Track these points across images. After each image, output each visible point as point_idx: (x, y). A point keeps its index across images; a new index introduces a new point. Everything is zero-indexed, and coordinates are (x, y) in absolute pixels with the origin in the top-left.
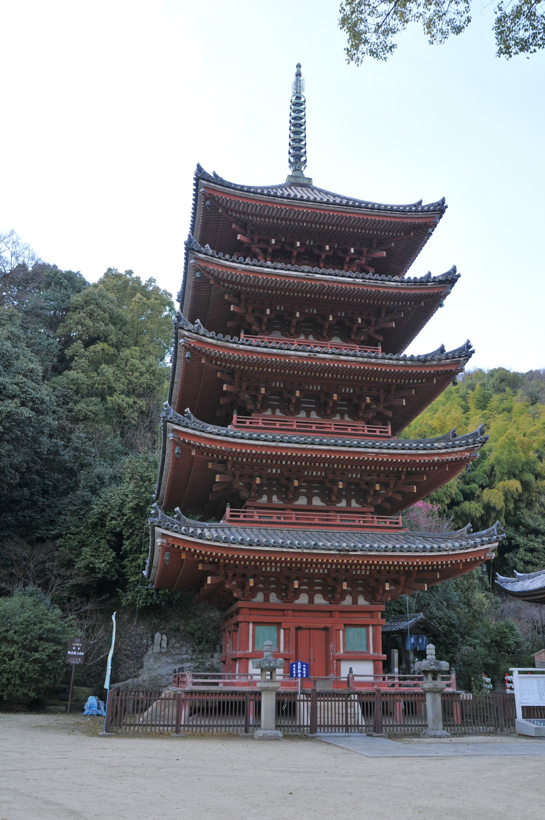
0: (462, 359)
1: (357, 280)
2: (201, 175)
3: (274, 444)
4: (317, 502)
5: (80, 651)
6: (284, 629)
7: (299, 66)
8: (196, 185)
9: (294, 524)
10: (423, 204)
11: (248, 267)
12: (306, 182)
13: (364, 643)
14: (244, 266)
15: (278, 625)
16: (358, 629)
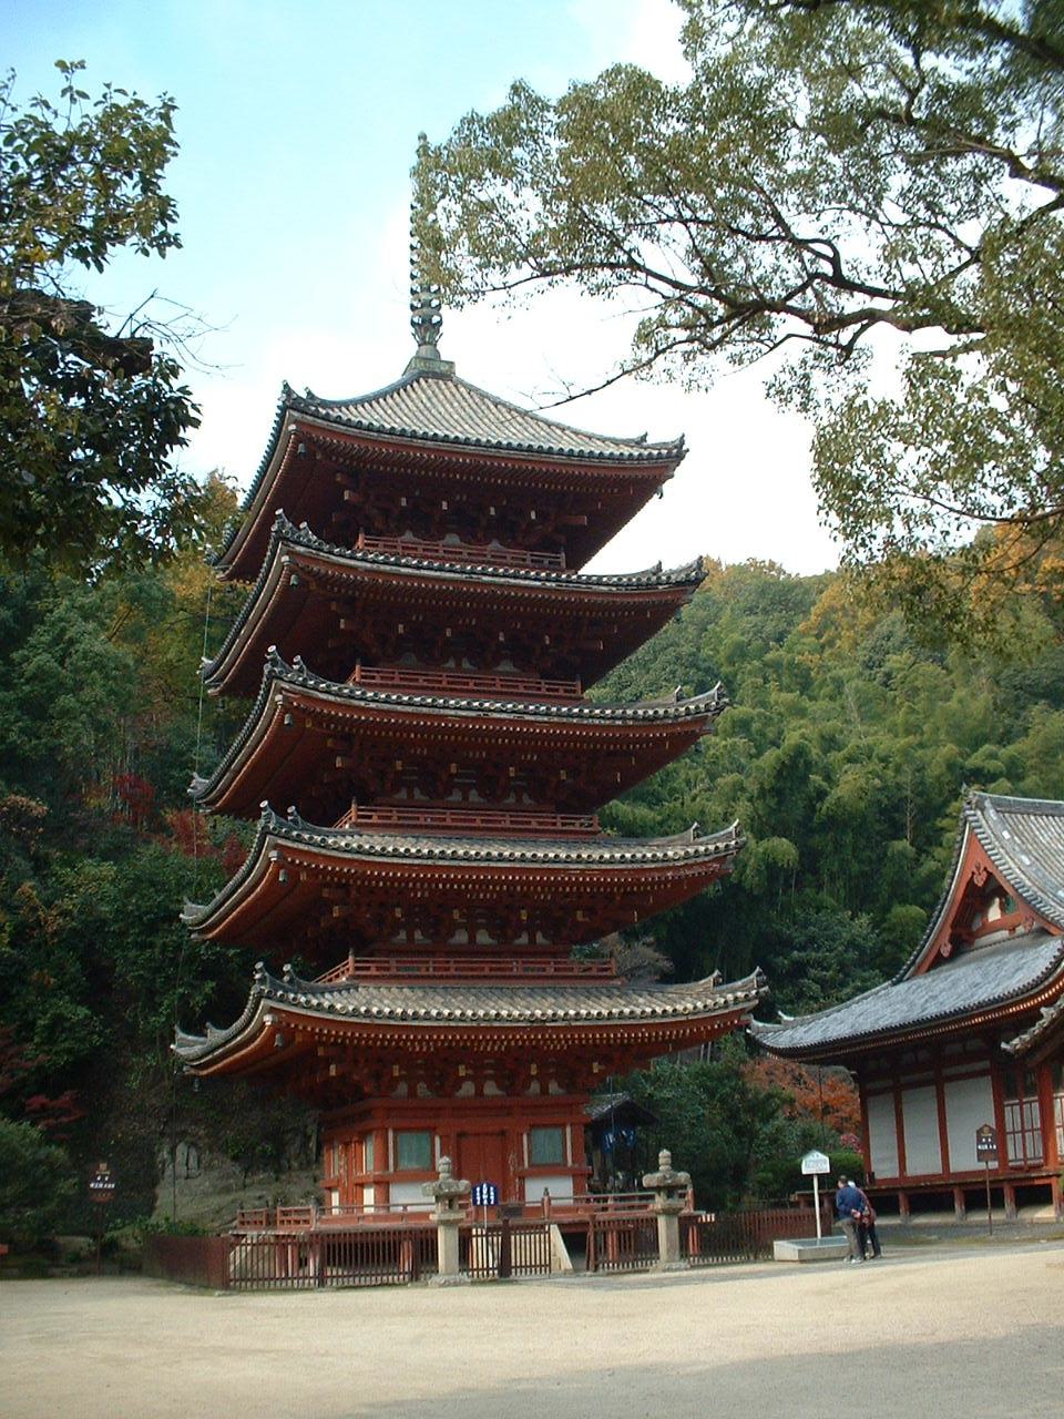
0: (710, 714)
1: (548, 584)
2: (294, 405)
3: (430, 862)
4: (483, 938)
5: (108, 1182)
6: (441, 1138)
8: (282, 416)
9: (454, 977)
10: (650, 441)
11: (375, 566)
12: (444, 368)
13: (559, 1152)
14: (369, 565)
15: (432, 1130)
16: (550, 1131)
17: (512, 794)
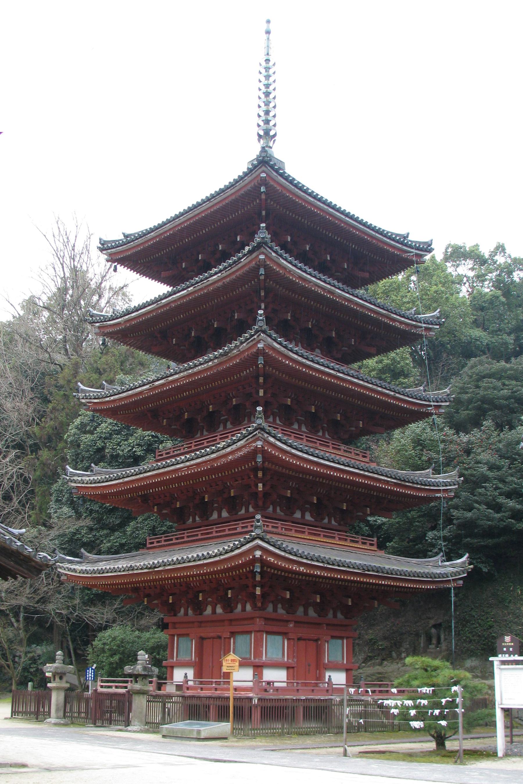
4: (308, 517)
7: (268, 22)
10: (410, 238)
17: (321, 431)
